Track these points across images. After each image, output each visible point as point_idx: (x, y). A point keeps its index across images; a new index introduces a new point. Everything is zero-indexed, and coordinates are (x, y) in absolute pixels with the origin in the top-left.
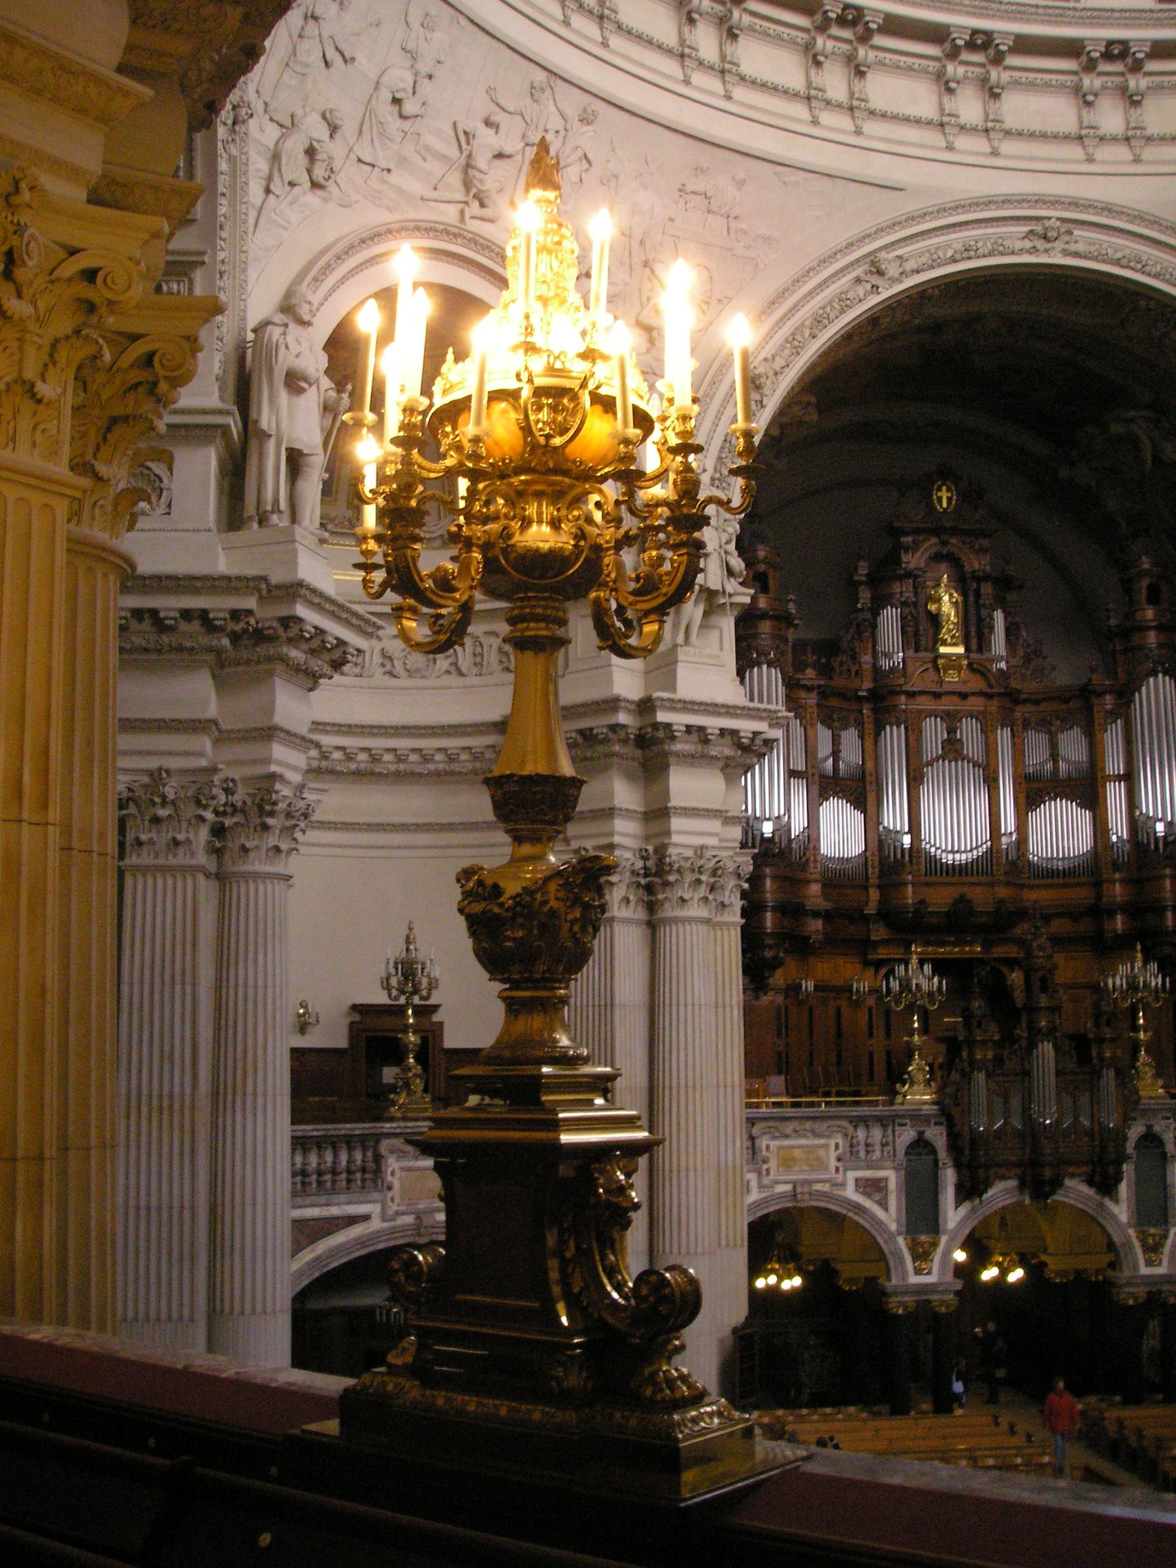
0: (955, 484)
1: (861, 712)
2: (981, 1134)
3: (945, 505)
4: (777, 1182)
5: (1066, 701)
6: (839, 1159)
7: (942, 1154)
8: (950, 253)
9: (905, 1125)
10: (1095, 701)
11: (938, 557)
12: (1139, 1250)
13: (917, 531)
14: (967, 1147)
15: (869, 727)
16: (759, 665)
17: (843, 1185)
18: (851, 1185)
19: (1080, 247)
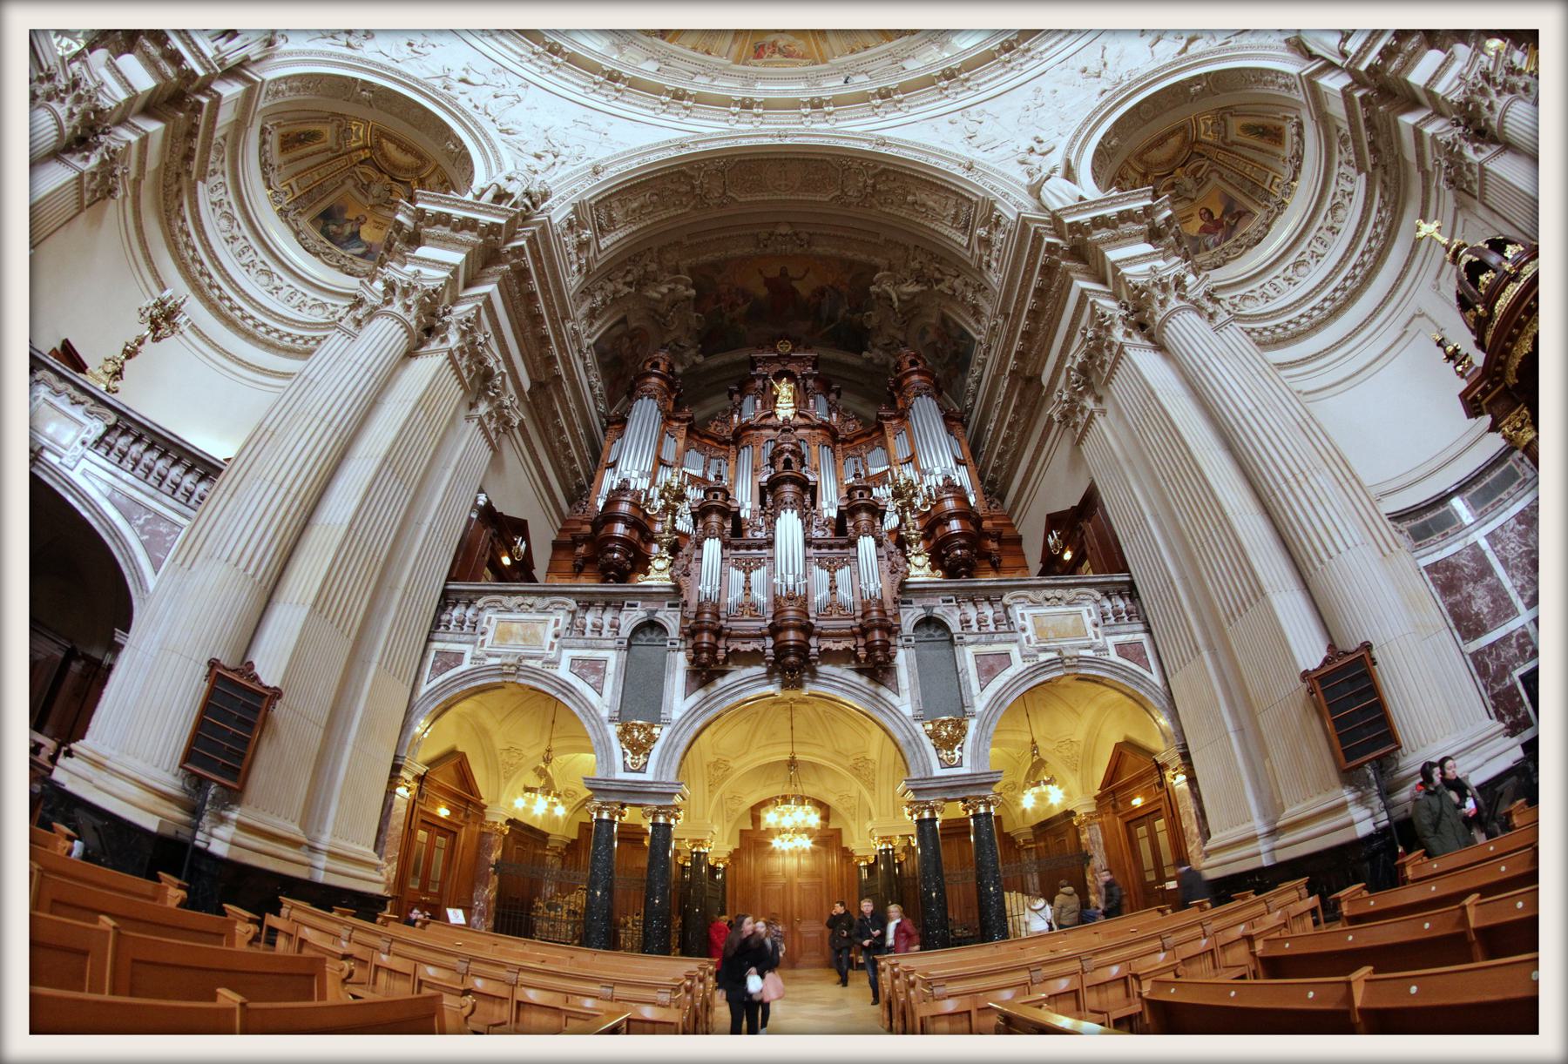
4: (489, 655)
6: (556, 636)
9: (635, 606)
12: (931, 750)
17: (555, 663)
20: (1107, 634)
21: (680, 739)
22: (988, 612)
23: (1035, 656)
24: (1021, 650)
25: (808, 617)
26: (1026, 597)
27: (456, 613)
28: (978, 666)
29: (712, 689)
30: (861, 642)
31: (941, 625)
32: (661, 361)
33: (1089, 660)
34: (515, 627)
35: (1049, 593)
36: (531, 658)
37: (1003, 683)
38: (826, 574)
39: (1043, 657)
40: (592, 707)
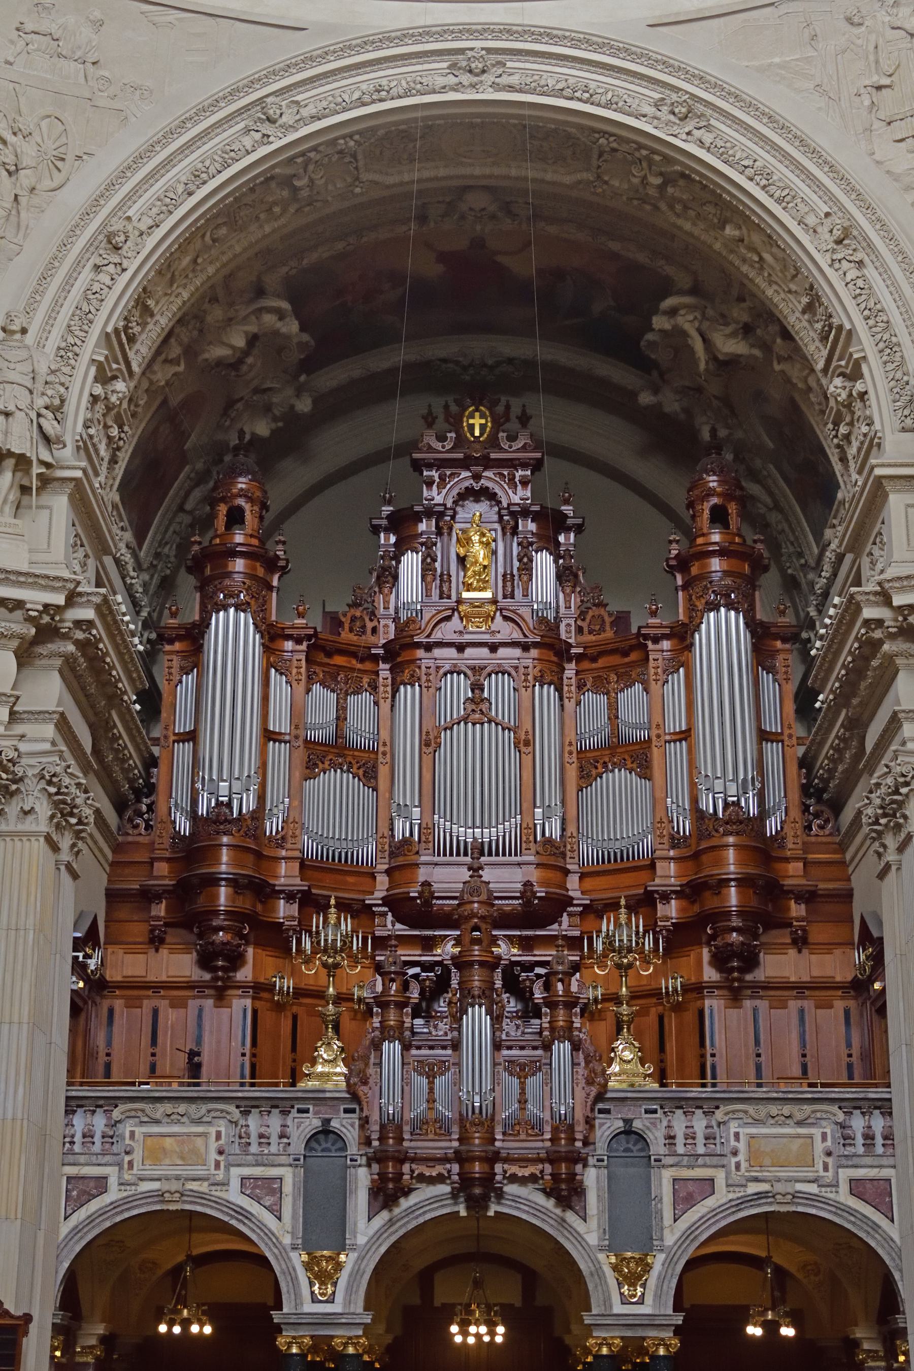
0: (490, 409)
1: (377, 673)
2: (391, 1121)
3: (477, 433)
4: (141, 1180)
5: (626, 654)
6: (221, 1153)
7: (353, 1149)
8: (356, 96)
9: (307, 1111)
10: (650, 646)
11: (468, 494)
13: (440, 464)
14: (375, 1136)
15: (385, 689)
16: (225, 608)
17: (225, 1184)
18: (235, 1184)
19: (514, 80)
20: (840, 1166)
21: (367, 1265)
22: (699, 1123)
23: (742, 1186)
24: (727, 1178)
25: (495, 1140)
26: (746, 1112)
27: (79, 1121)
28: (675, 1192)
29: (397, 1211)
30: (548, 1169)
31: (641, 1138)
32: (241, 502)
33: (811, 1198)
34: (168, 1141)
35: (774, 1109)
36: (194, 1180)
37: (700, 1215)
38: (516, 1081)
39: (753, 1188)
40: (273, 1234)
